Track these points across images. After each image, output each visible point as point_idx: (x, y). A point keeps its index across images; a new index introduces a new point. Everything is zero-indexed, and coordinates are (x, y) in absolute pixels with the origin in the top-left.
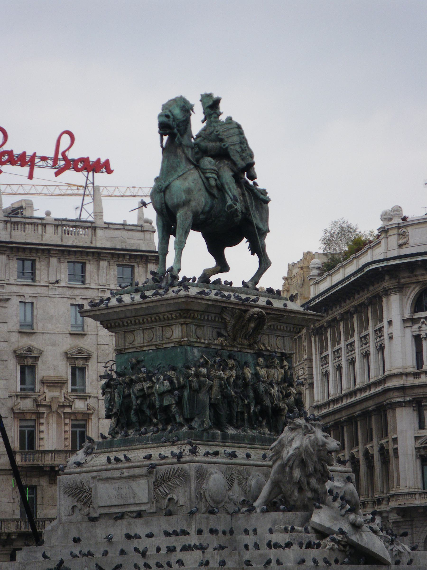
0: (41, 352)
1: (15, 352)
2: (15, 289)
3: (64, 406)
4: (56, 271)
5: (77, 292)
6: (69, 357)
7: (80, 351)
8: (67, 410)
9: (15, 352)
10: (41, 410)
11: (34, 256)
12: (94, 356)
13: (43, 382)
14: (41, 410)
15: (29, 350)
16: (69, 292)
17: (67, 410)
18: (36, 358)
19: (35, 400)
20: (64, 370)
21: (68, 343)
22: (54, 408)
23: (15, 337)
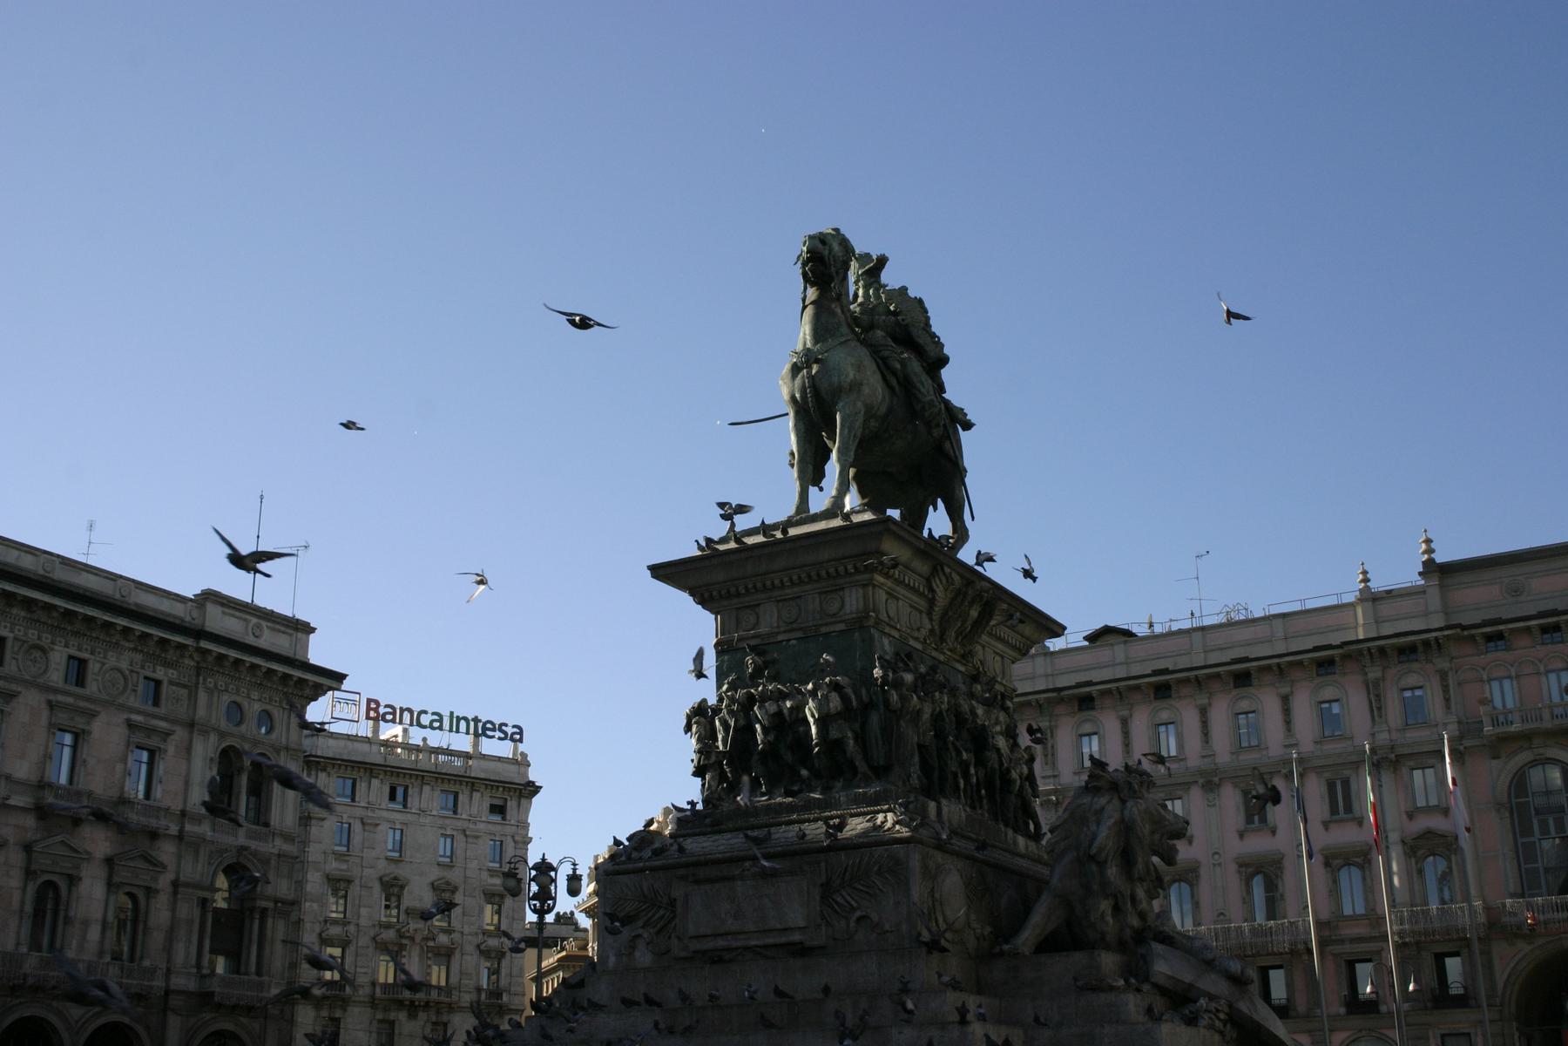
0: (408, 882)
1: (381, 879)
2: (385, 814)
3: (427, 939)
4: (430, 799)
5: (447, 822)
6: (434, 887)
7: (448, 883)
8: (431, 944)
9: (381, 879)
10: (404, 941)
11: (408, 781)
12: (461, 890)
13: (408, 912)
14: (404, 941)
15: (395, 878)
16: (440, 822)
17: (431, 944)
18: (402, 887)
19: (398, 931)
20: (427, 900)
21: (435, 874)
22: (418, 939)
23: (382, 864)
